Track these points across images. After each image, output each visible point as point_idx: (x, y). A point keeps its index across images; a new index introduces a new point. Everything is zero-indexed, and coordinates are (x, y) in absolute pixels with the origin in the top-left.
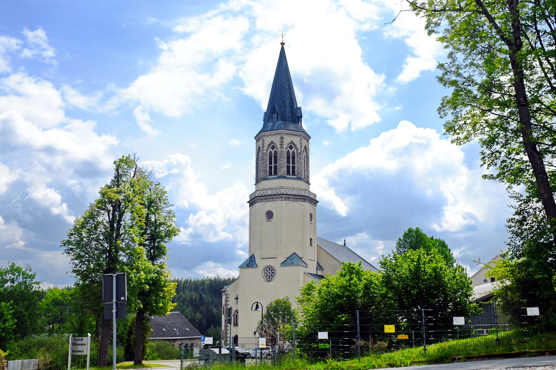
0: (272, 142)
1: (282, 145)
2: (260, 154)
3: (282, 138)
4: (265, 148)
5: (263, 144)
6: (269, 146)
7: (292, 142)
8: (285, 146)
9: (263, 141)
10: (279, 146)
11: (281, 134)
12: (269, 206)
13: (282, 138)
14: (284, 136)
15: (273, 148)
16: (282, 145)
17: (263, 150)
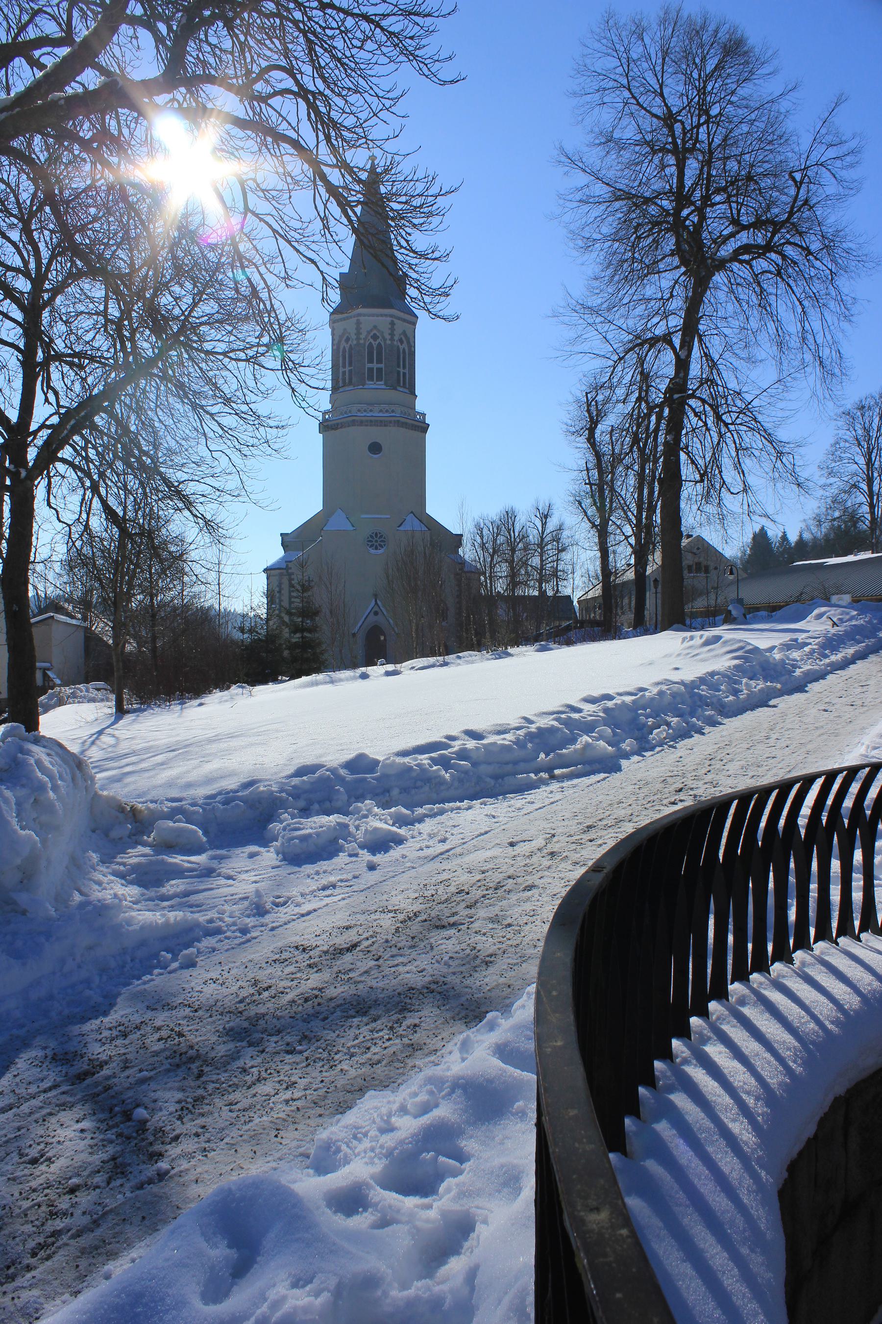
0: (375, 327)
1: (392, 335)
2: (343, 344)
3: (392, 324)
4: (362, 336)
5: (358, 329)
6: (369, 332)
7: (404, 333)
8: (396, 338)
9: (358, 323)
10: (388, 337)
11: (391, 316)
12: (376, 434)
13: (392, 324)
14: (396, 321)
15: (375, 337)
16: (392, 335)
17: (358, 339)
